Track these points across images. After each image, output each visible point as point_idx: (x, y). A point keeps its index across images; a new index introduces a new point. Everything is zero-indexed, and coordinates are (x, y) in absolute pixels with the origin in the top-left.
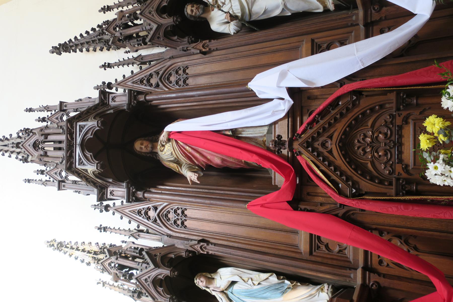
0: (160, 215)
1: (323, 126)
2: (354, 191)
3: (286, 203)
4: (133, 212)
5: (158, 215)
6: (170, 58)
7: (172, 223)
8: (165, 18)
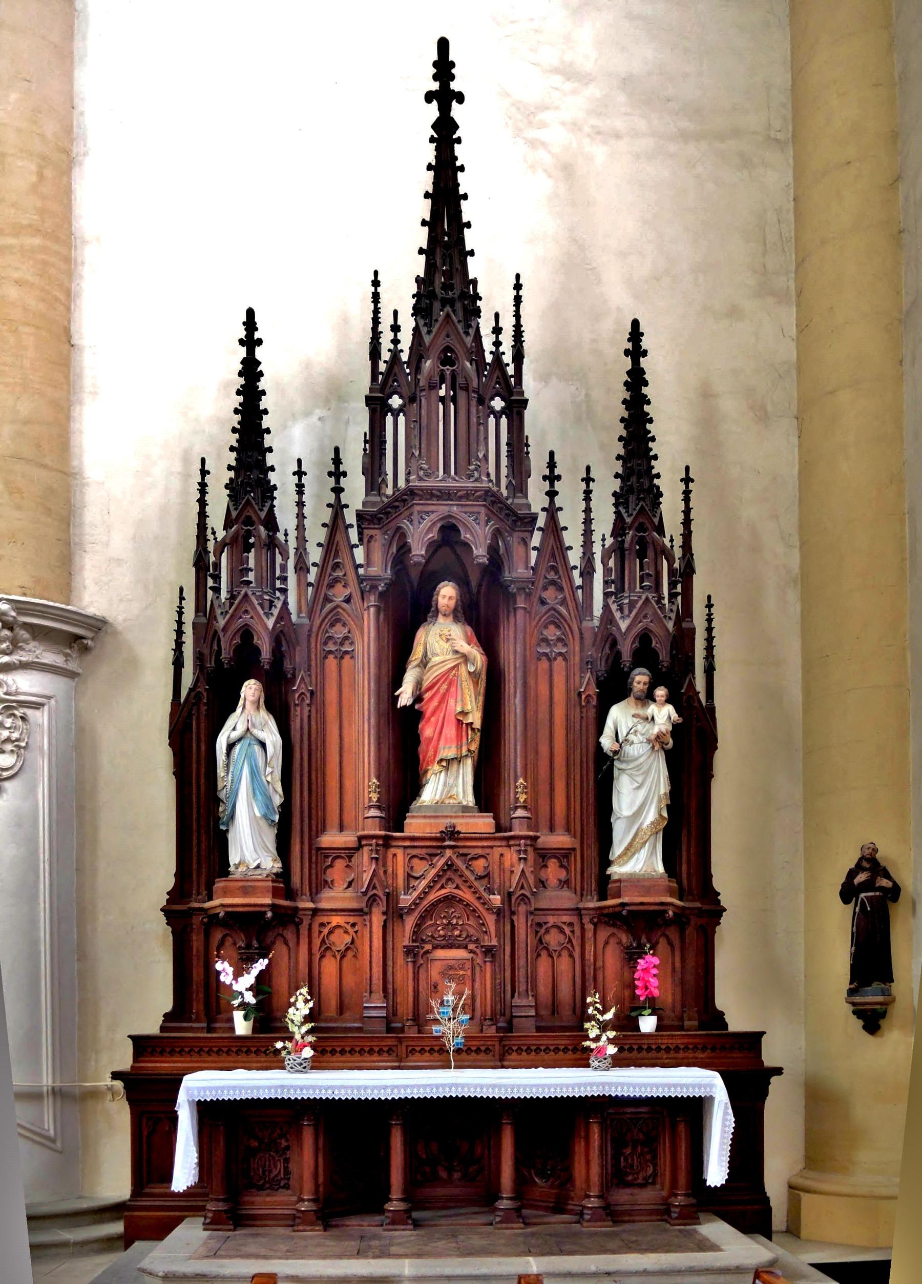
8: (633, 642)
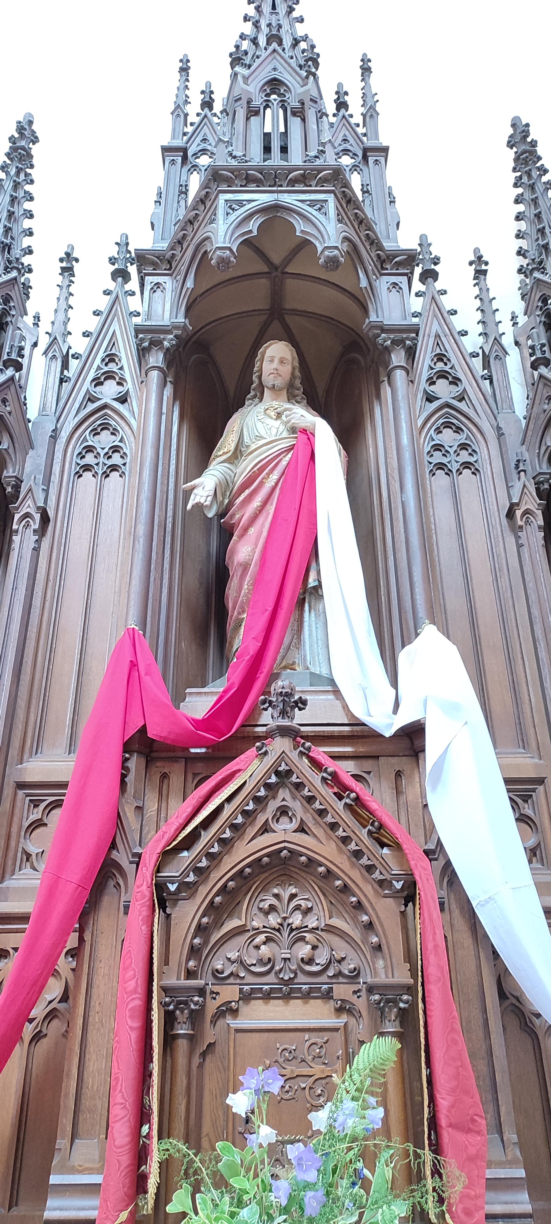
0: (106, 411)
1: (329, 809)
2: (172, 888)
3: (142, 723)
4: (113, 344)
5: (105, 406)
6: (499, 428)
7: (87, 441)
